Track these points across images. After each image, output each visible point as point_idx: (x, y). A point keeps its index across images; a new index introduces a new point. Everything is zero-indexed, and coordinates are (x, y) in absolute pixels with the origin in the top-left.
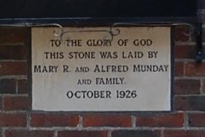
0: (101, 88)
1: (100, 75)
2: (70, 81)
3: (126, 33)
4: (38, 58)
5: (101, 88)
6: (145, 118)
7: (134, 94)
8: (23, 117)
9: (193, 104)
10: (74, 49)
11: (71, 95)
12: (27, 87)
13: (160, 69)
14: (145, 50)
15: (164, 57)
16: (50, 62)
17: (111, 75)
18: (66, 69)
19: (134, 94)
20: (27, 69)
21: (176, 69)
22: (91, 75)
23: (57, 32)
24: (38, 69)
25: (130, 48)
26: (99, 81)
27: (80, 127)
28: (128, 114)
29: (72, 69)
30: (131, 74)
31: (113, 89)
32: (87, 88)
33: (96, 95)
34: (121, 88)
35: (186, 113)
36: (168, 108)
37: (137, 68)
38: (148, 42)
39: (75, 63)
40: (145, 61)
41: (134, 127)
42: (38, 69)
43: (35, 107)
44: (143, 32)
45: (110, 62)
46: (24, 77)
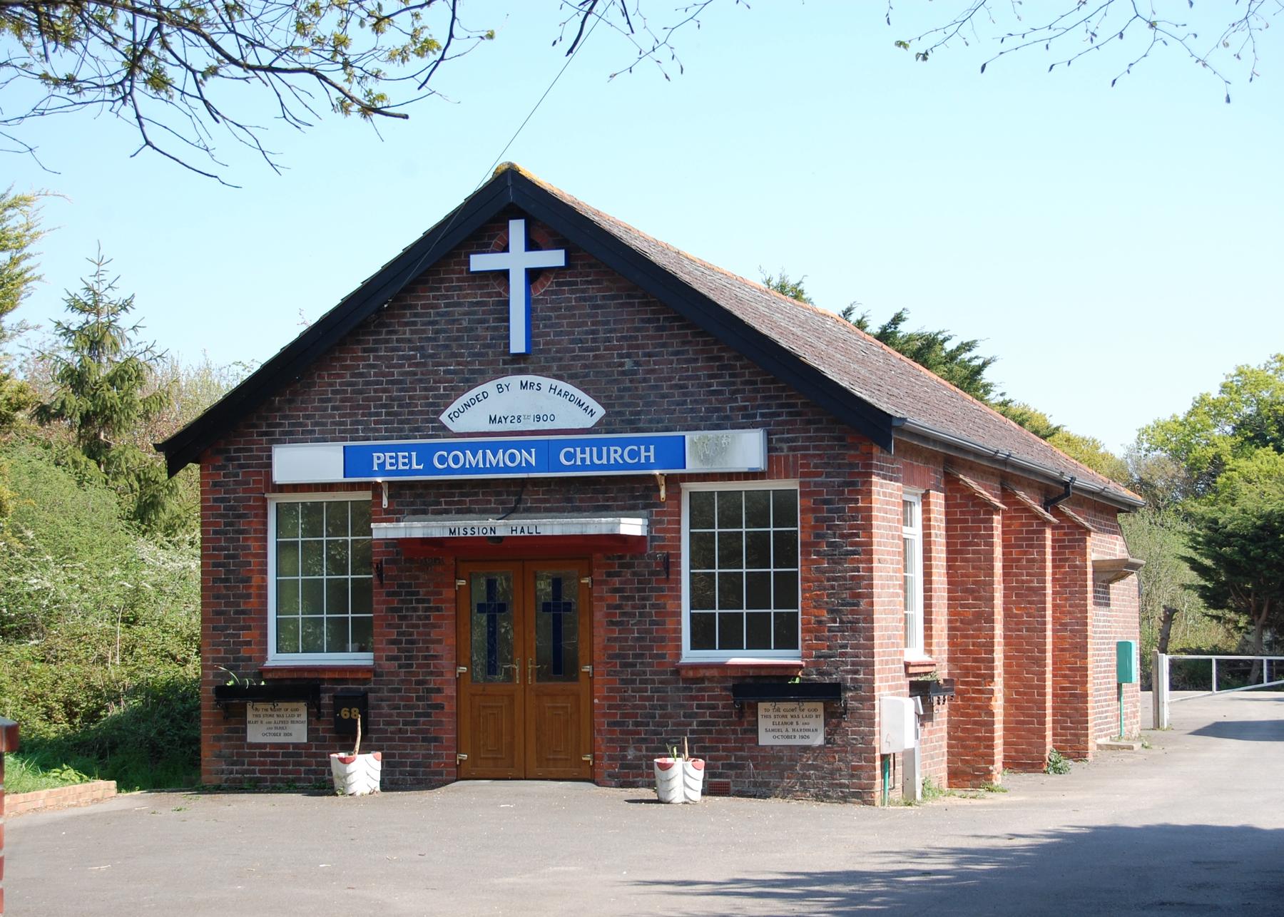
0: (277, 731)
1: (276, 725)
2: (263, 728)
3: (281, 705)
4: (250, 717)
5: (277, 731)
6: (296, 746)
7: (291, 734)
8: (243, 745)
9: (317, 739)
10: (265, 713)
11: (264, 735)
12: (245, 731)
13: (302, 722)
14: (296, 713)
15: (304, 717)
16: (254, 719)
17: (281, 725)
18: (262, 722)
19: (291, 734)
20: (245, 722)
21: (309, 723)
22: (272, 725)
23: (260, 706)
24: (249, 722)
25: (289, 712)
26: (276, 728)
27: (268, 750)
28: (288, 744)
29: (264, 722)
30: (290, 725)
31: (282, 732)
32: (270, 731)
33: (275, 735)
34: (285, 731)
35: (314, 744)
36: (306, 741)
37: (292, 722)
38: (297, 710)
39: (265, 720)
40: (296, 719)
41: (291, 750)
42: (249, 722)
43: (248, 740)
44: (295, 705)
45: (281, 719)
46: (244, 726)
